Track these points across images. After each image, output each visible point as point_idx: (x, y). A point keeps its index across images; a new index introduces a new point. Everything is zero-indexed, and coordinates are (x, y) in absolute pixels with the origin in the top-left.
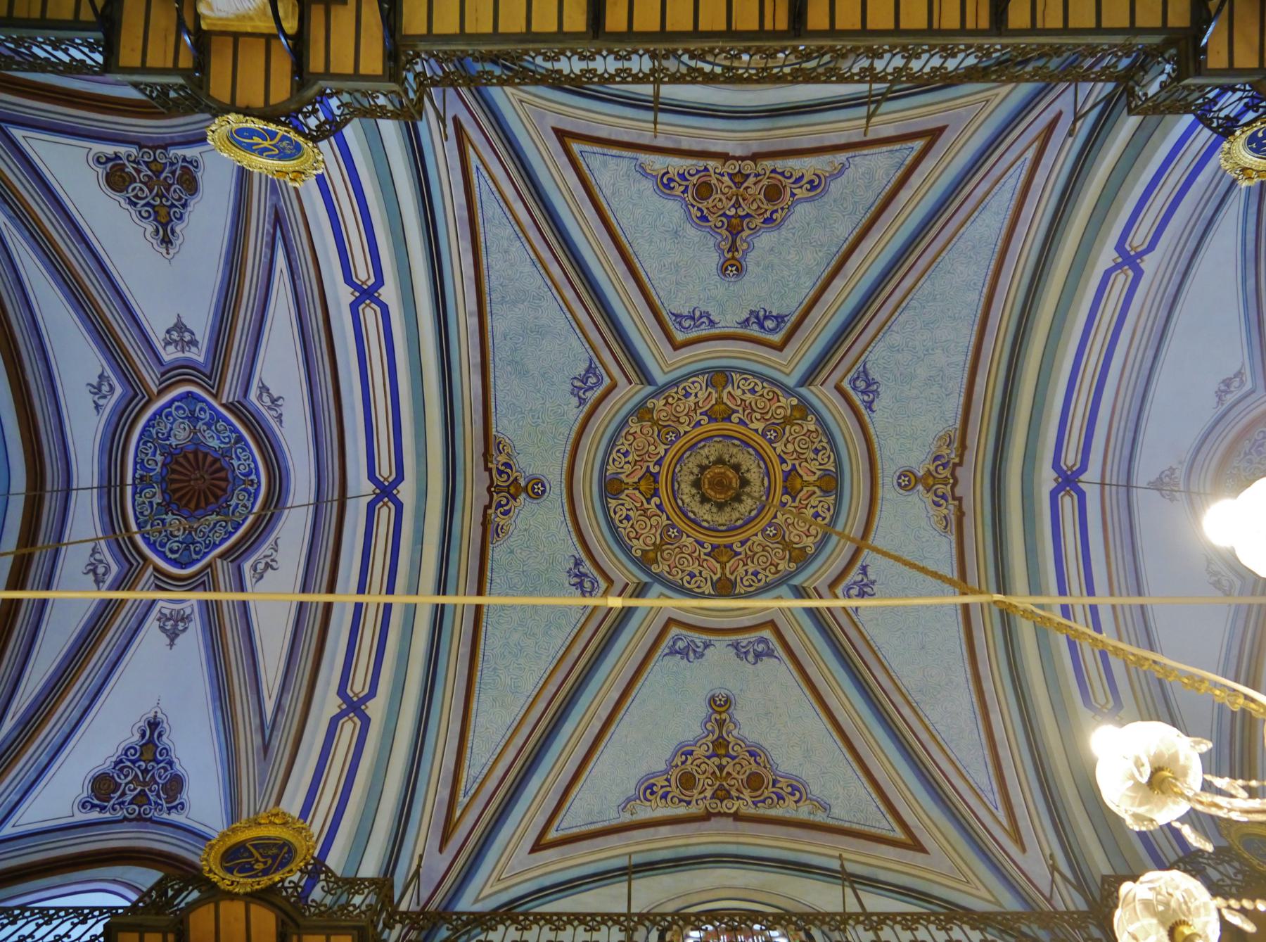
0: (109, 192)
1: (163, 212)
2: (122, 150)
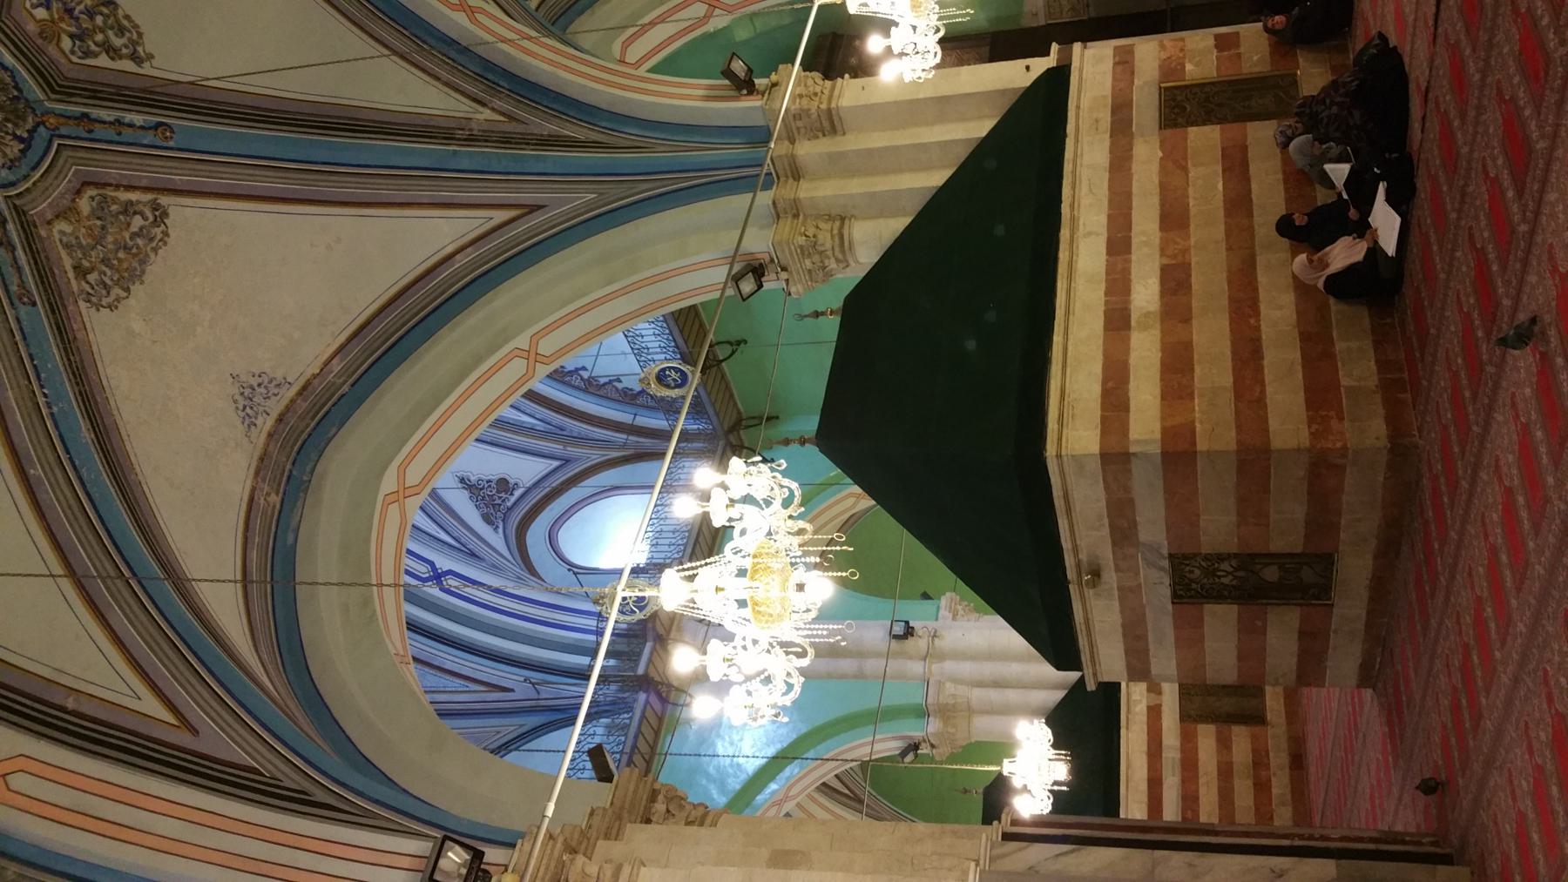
0: (502, 476)
1: (476, 492)
2: (513, 499)
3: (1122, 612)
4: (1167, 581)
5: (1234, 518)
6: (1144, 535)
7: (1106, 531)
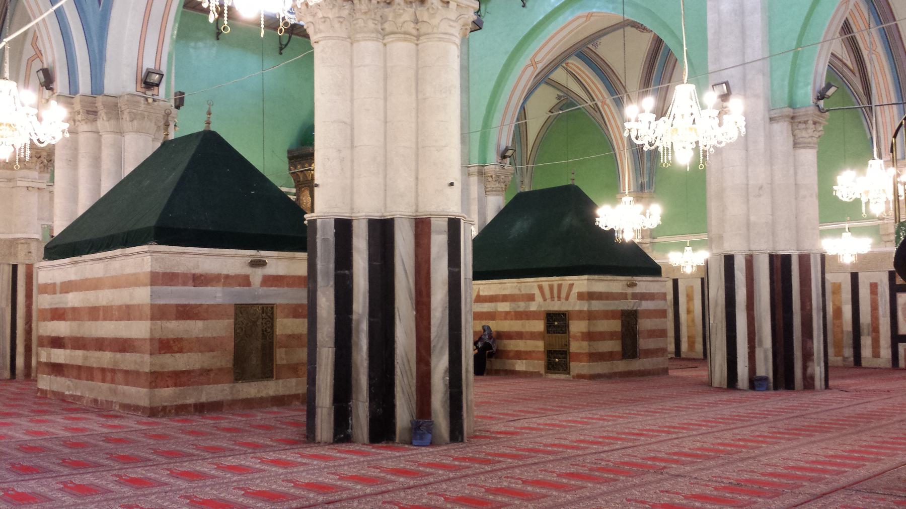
3: (617, 293)
4: (629, 308)
5: (649, 328)
6: (644, 302)
7: (645, 291)
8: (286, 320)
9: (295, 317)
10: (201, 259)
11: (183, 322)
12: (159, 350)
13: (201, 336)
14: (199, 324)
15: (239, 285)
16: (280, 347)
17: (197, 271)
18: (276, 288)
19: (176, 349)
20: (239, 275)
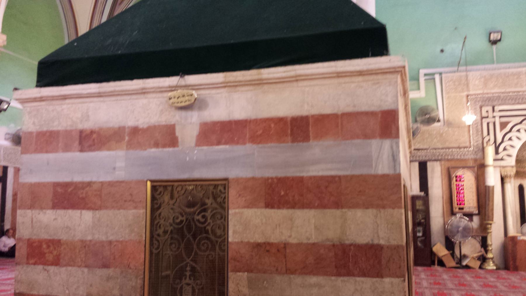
8: (249, 213)
9: (269, 205)
10: (92, 105)
11: (61, 212)
12: (28, 258)
13: (89, 238)
14: (87, 216)
15: (156, 145)
16: (237, 270)
17: (87, 126)
18: (227, 147)
19: (50, 257)
20: (155, 126)
